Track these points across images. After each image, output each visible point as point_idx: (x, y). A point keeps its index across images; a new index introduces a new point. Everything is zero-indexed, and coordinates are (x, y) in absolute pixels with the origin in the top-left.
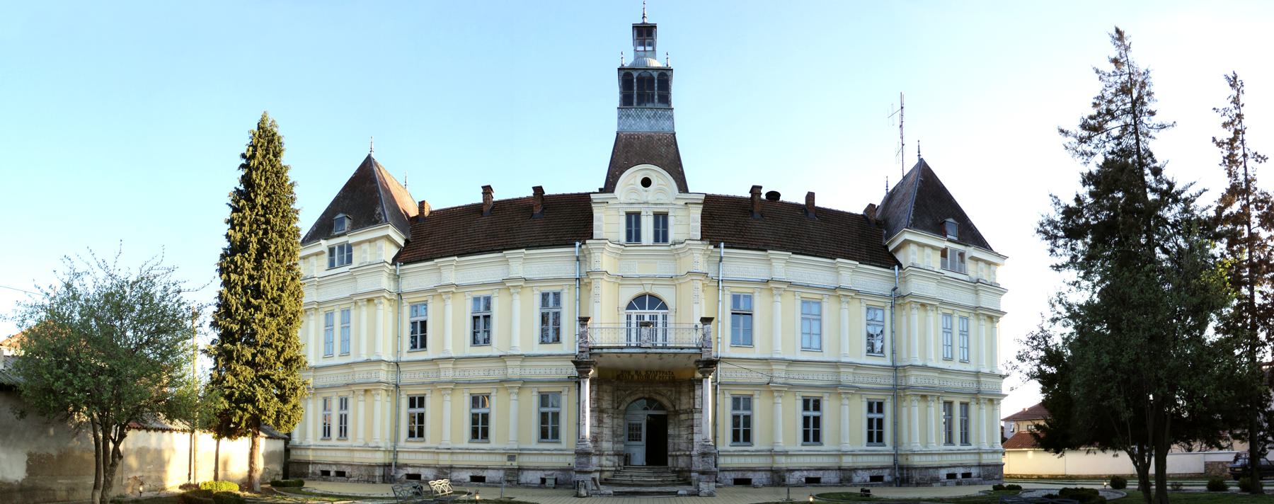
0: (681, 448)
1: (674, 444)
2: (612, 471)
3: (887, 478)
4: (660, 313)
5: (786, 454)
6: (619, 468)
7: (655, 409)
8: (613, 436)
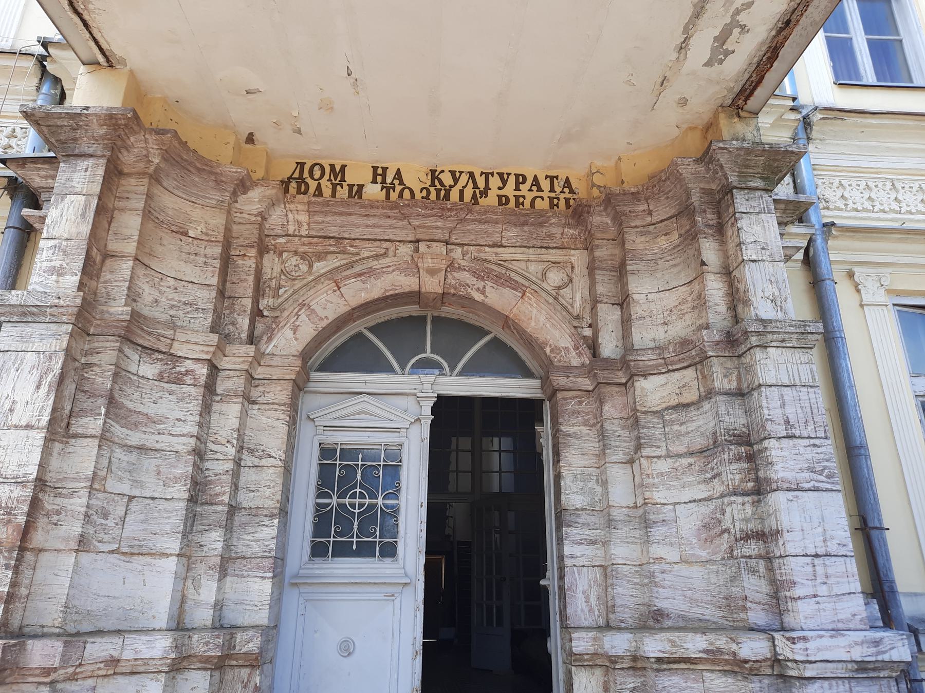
1: (607, 571)
7: (469, 370)
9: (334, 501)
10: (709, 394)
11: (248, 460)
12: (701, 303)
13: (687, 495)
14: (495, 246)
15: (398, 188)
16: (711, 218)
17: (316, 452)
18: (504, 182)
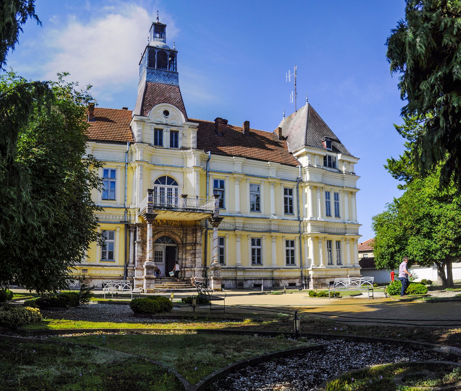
0: (187, 266)
3: (298, 284)
4: (174, 187)
5: (244, 270)
7: (169, 243)
10: (192, 249)
12: (193, 240)
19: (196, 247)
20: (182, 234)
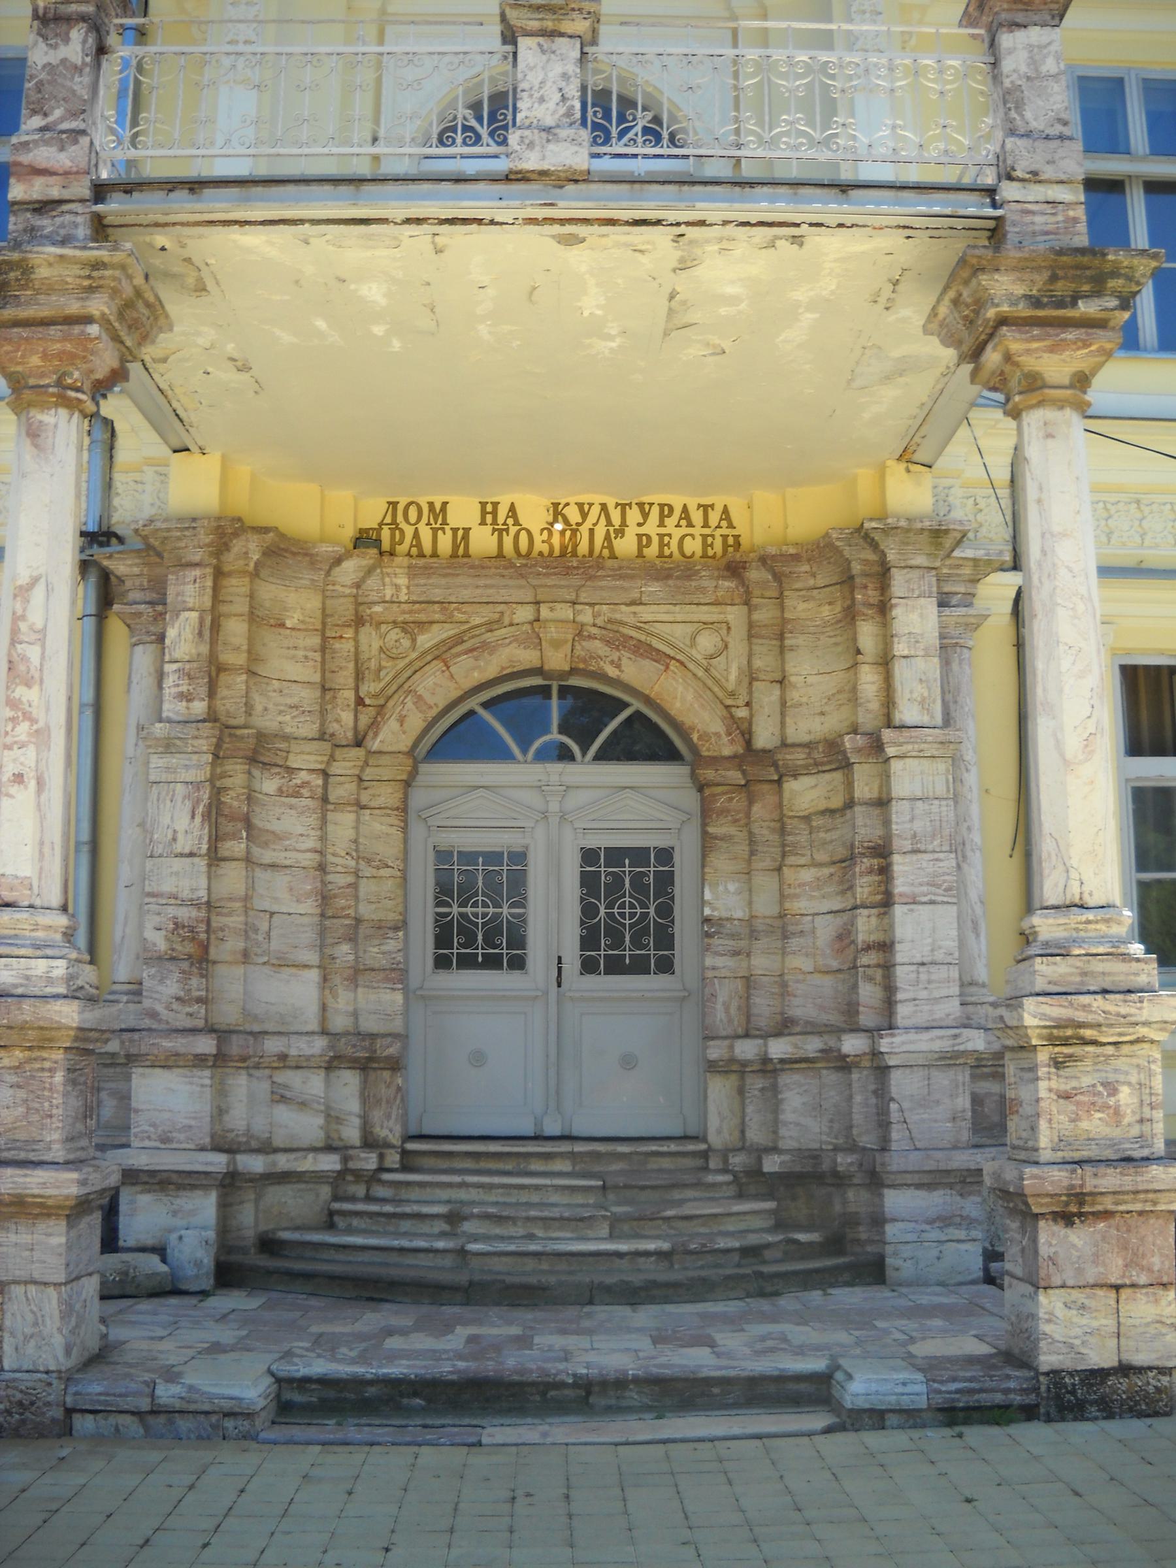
0: (802, 1008)
1: (748, 981)
2: (317, 1177)
6: (369, 1161)
8: (322, 932)
9: (455, 910)
11: (368, 871)
12: (852, 695)
13: (826, 906)
14: (633, 603)
15: (513, 530)
16: (873, 595)
17: (431, 855)
18: (645, 515)
19: (885, 777)
20: (738, 645)
